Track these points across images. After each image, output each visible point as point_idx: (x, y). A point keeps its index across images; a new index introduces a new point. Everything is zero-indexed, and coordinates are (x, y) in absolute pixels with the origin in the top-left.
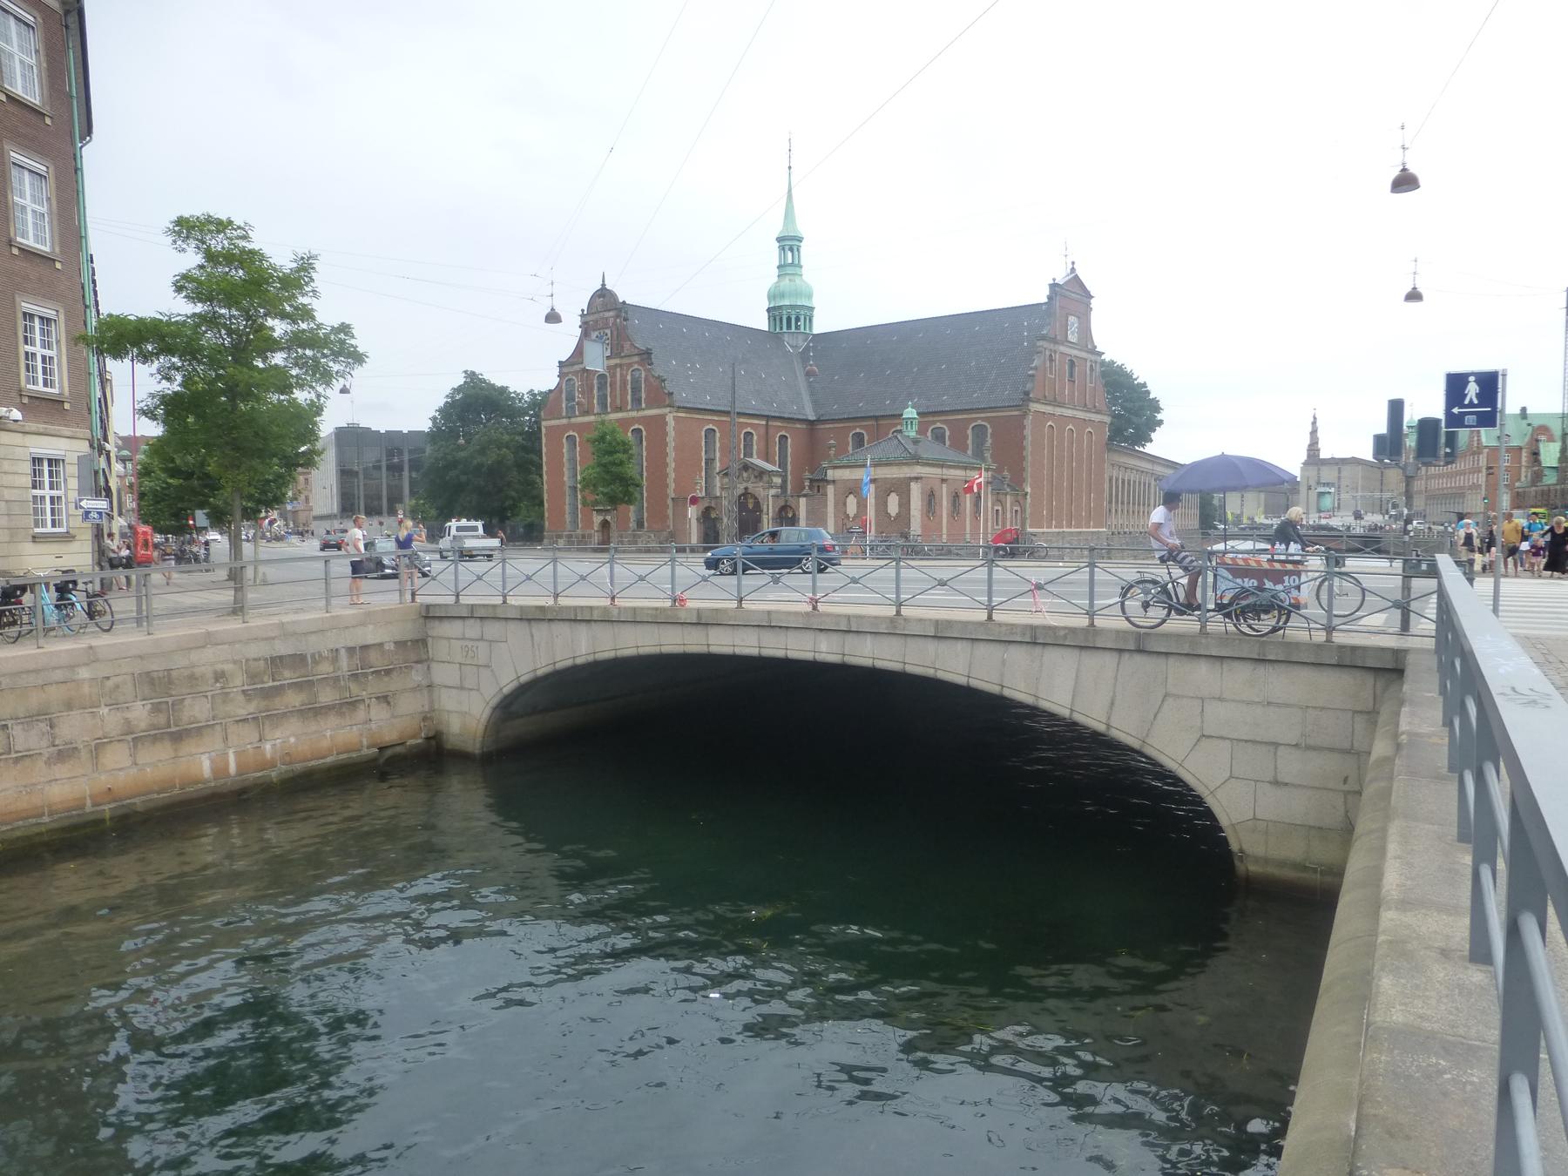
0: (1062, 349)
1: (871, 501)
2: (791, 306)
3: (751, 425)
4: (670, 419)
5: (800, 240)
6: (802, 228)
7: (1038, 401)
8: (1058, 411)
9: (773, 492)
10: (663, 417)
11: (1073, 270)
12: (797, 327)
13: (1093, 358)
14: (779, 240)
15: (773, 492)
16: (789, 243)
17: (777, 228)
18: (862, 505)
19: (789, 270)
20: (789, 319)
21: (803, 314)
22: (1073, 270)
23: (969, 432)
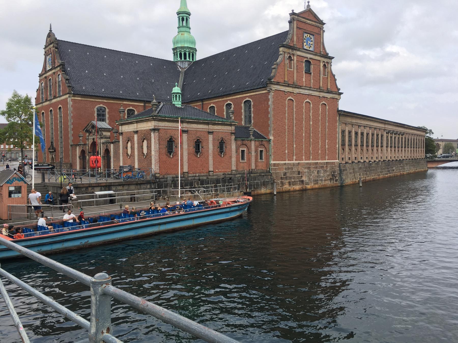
0: (299, 53)
1: (136, 146)
2: (182, 48)
3: (133, 106)
4: (69, 100)
5: (189, 14)
6: (190, 8)
7: (278, 84)
8: (296, 91)
9: (103, 140)
10: (67, 99)
11: (308, 6)
12: (185, 58)
13: (326, 60)
14: (178, 13)
15: (103, 140)
16: (184, 17)
17: (177, 7)
18: (132, 148)
19: (182, 29)
20: (181, 54)
21: (193, 51)
22: (308, 6)
23: (243, 105)
